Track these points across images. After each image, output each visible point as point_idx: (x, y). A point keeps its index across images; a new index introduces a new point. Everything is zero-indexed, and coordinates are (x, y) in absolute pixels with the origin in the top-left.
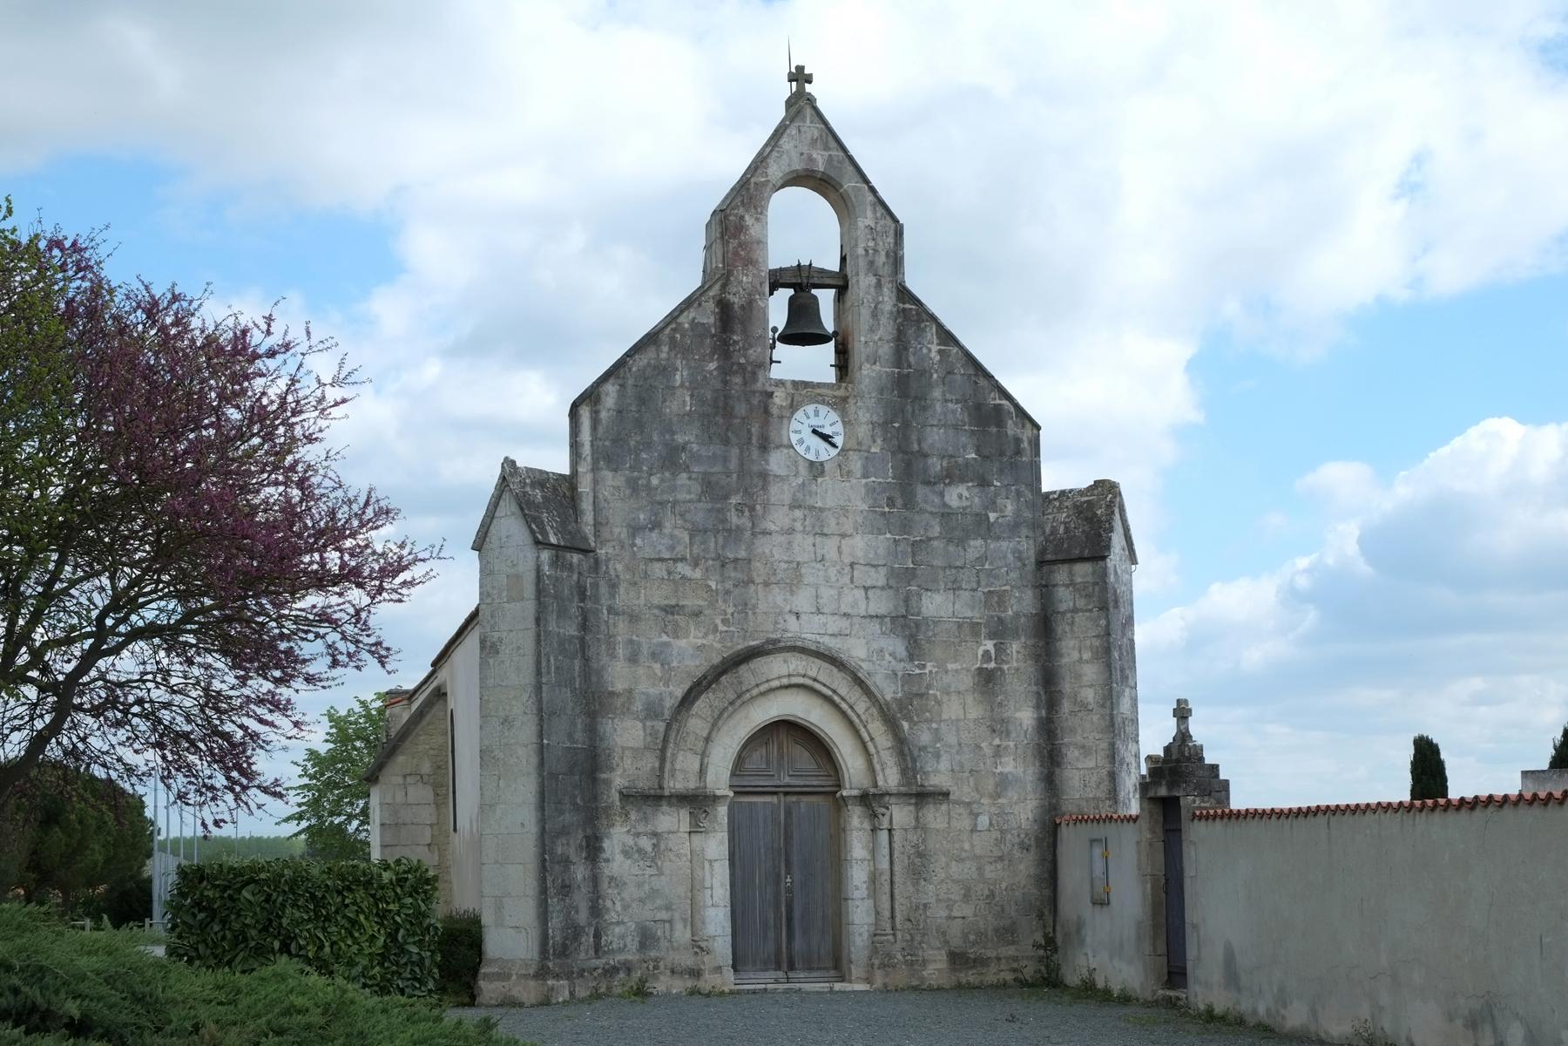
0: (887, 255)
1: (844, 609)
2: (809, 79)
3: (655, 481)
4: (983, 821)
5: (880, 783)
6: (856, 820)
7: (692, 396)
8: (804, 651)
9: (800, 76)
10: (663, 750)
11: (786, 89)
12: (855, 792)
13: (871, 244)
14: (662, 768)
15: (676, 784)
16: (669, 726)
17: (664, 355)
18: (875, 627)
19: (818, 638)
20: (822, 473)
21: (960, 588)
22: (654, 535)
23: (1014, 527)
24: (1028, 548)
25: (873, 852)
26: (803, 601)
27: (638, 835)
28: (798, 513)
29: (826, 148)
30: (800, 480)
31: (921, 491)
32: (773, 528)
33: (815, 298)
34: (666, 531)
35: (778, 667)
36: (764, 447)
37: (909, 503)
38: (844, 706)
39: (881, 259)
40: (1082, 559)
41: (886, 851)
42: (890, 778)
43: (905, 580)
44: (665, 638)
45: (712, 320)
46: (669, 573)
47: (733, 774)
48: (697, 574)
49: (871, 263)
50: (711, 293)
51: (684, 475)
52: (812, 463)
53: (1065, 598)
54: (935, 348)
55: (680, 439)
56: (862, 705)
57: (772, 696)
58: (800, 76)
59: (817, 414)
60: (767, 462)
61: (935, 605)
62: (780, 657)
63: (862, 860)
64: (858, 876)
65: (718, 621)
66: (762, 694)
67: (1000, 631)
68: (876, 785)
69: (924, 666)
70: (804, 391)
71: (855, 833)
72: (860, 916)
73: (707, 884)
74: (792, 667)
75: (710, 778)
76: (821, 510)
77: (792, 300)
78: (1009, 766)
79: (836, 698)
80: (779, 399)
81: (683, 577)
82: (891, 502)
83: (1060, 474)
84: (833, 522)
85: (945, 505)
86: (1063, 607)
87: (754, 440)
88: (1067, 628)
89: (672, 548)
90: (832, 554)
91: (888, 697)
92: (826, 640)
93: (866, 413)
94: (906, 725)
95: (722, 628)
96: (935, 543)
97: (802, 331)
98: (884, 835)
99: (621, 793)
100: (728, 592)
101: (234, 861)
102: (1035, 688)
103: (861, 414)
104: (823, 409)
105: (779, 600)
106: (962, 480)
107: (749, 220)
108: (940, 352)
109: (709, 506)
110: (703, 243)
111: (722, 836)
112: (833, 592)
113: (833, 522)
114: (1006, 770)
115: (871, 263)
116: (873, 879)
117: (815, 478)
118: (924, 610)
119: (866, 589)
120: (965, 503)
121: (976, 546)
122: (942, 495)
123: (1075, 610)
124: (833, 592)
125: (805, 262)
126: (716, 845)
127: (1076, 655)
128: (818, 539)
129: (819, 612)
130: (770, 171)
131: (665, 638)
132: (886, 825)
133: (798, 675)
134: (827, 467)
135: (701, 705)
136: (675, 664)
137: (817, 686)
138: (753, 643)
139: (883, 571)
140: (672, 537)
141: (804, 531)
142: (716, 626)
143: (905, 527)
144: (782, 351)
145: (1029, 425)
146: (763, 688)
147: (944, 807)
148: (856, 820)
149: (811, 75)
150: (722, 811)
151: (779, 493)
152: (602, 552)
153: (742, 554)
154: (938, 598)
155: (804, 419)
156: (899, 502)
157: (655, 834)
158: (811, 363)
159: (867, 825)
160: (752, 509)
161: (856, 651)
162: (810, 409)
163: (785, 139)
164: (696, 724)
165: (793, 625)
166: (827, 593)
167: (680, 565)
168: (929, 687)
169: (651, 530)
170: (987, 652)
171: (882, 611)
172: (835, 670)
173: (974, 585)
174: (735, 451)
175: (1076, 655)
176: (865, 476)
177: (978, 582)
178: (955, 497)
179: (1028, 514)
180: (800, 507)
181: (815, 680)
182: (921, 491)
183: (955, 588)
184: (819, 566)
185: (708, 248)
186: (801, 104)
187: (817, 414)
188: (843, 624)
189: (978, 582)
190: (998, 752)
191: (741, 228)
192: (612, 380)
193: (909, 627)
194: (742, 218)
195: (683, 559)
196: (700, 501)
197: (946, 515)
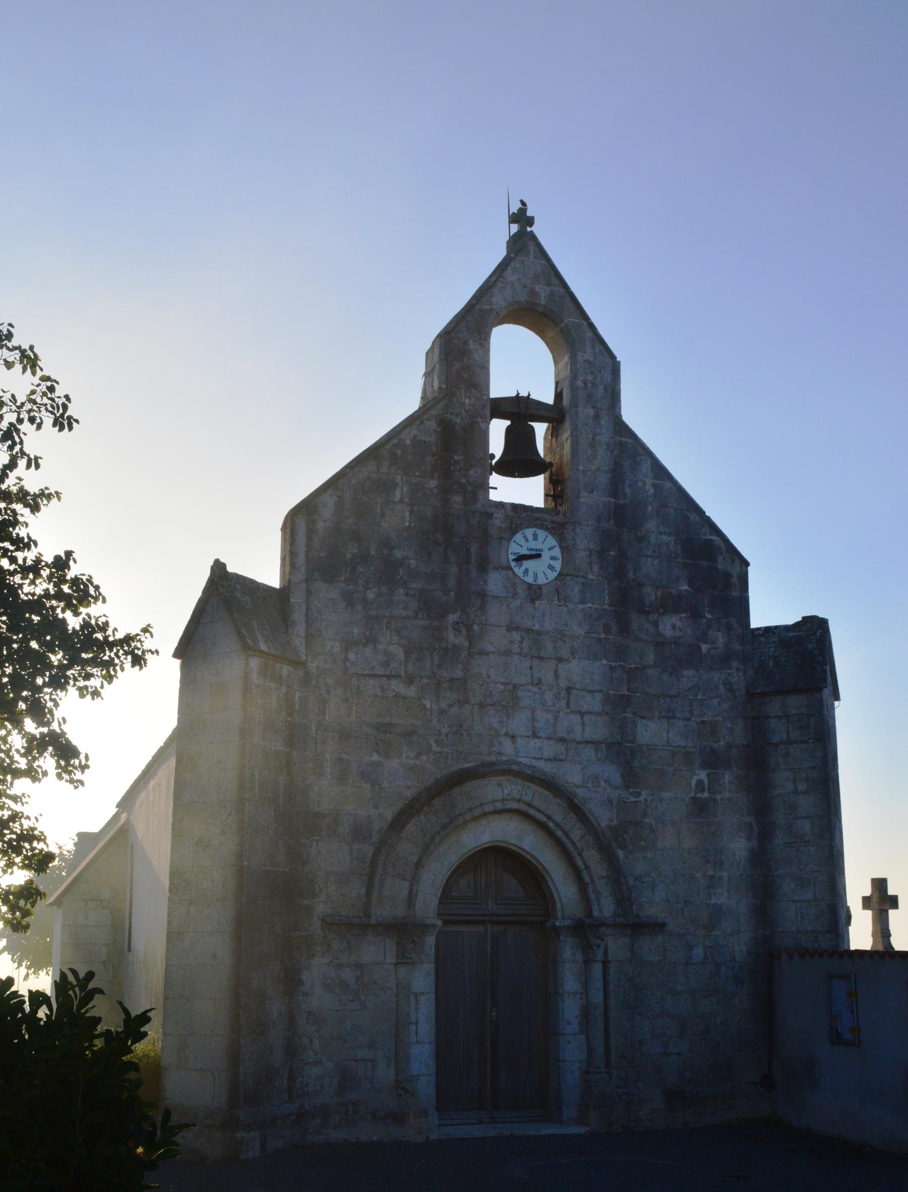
0: (605, 390)
1: (561, 733)
2: (530, 221)
3: (371, 595)
4: (699, 952)
5: (596, 913)
6: (569, 953)
7: (411, 512)
8: (518, 774)
9: (522, 218)
10: (371, 876)
11: (504, 231)
12: (567, 923)
13: (590, 378)
14: (368, 894)
15: (383, 912)
16: (377, 852)
17: (384, 469)
18: (589, 753)
19: (534, 763)
20: (539, 597)
21: (674, 717)
22: (368, 651)
23: (725, 660)
24: (738, 679)
25: (586, 985)
26: (519, 723)
27: (340, 966)
28: (516, 636)
29: (549, 284)
30: (518, 602)
31: (636, 620)
32: (490, 649)
33: (532, 428)
34: (381, 647)
35: (493, 790)
36: (484, 566)
37: (624, 628)
38: (559, 833)
39: (601, 391)
40: (796, 691)
41: (600, 984)
42: (606, 907)
43: (621, 705)
44: (375, 757)
45: (433, 438)
46: (383, 690)
47: (441, 902)
48: (411, 692)
49: (590, 396)
50: (433, 412)
51: (401, 591)
52: (530, 585)
53: (778, 730)
54: (649, 482)
55: (398, 554)
56: (577, 833)
57: (484, 821)
58: (522, 218)
59: (535, 537)
60: (486, 582)
61: (649, 732)
62: (494, 780)
63: (575, 994)
64: (570, 1009)
65: (432, 742)
66: (475, 819)
67: (713, 761)
68: (590, 914)
69: (639, 794)
70: (520, 514)
71: (567, 965)
72: (572, 1051)
73: (413, 1020)
74: (506, 791)
75: (419, 905)
76: (539, 633)
77: (509, 431)
78: (722, 898)
79: (551, 824)
80: (498, 521)
81: (397, 695)
82: (607, 629)
83: (770, 606)
84: (549, 646)
85: (659, 634)
86: (775, 739)
87: (473, 561)
88: (781, 759)
89: (386, 664)
90: (549, 677)
91: (604, 824)
92: (541, 764)
93: (584, 541)
94: (621, 853)
95: (435, 748)
96: (650, 672)
97: (520, 461)
98: (597, 969)
99: (323, 920)
100: (442, 712)
101: (879, 929)
102: (748, 819)
103: (578, 541)
104: (542, 534)
105: (495, 722)
106: (676, 611)
107: (472, 345)
108: (654, 485)
109: (425, 623)
110: (423, 370)
111: (428, 967)
112: (549, 716)
113: (549, 646)
114: (720, 902)
115: (590, 396)
116: (586, 1013)
117: (533, 601)
118: (638, 737)
119: (582, 714)
120: (678, 634)
121: (689, 676)
122: (656, 624)
123: (789, 742)
124: (549, 716)
125: (524, 394)
126: (422, 979)
127: (790, 787)
128: (536, 662)
129: (535, 735)
130: (494, 300)
131: (375, 757)
132: (600, 956)
133: (513, 799)
134: (545, 591)
135: (412, 828)
136: (385, 785)
137: (532, 812)
138: (466, 765)
139: (599, 697)
140: (386, 653)
141: (520, 654)
142: (430, 747)
143: (620, 653)
144: (495, 479)
145: (737, 562)
146: (477, 812)
147: (660, 938)
148: (569, 953)
149: (532, 218)
150: (430, 940)
151: (496, 614)
152: (313, 666)
153: (459, 673)
154: (653, 726)
155: (523, 542)
156: (614, 629)
157: (359, 966)
158: (529, 491)
159: (579, 957)
160: (469, 628)
161: (572, 776)
162: (529, 532)
163: (509, 271)
164: (406, 849)
165: (507, 747)
166: (543, 717)
167: (394, 682)
168: (645, 814)
169: (365, 645)
170: (700, 783)
171: (598, 737)
172: (550, 796)
173: (688, 715)
174: (454, 569)
175: (790, 787)
176: (583, 602)
177: (691, 712)
178: (669, 626)
179: (737, 647)
180: (517, 629)
181: (530, 805)
182: (636, 620)
183: (670, 716)
184: (535, 689)
185: (427, 375)
186: (523, 241)
187: (535, 537)
188: (560, 748)
189: (691, 712)
190: (712, 883)
191: (464, 352)
192: (329, 492)
193: (622, 752)
194: (466, 342)
195: (397, 677)
196: (416, 618)
197: (660, 644)
